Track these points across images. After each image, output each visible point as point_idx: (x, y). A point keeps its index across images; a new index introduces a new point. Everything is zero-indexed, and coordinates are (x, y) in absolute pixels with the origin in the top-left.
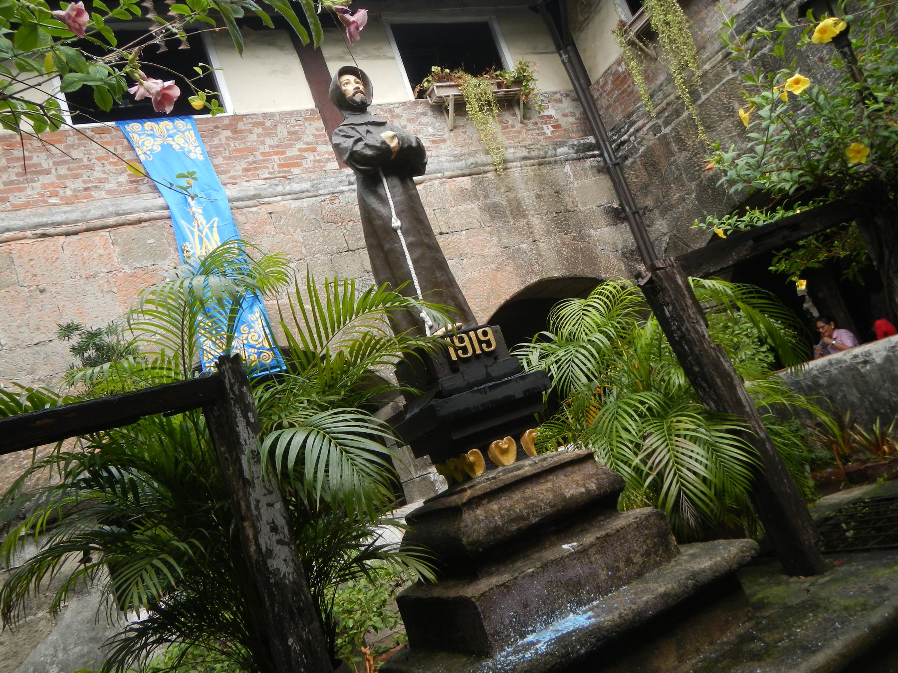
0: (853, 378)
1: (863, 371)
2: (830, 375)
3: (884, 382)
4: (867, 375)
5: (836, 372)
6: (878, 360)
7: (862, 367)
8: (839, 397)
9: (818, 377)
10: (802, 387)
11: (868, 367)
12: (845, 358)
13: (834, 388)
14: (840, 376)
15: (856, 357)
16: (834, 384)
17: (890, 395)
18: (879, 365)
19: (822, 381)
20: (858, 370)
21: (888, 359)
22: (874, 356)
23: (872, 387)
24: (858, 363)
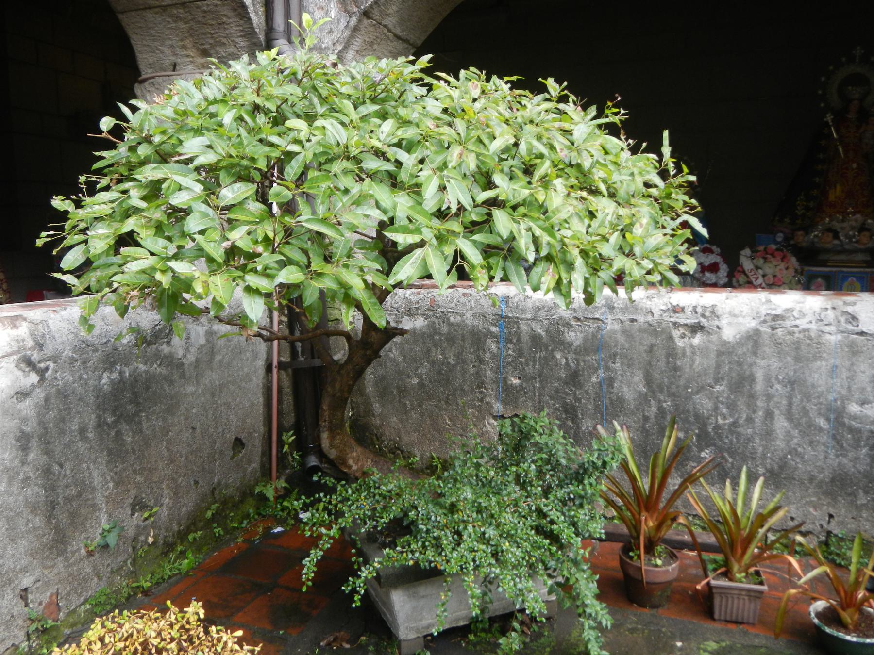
0: (651, 349)
1: (680, 343)
2: (599, 329)
3: (717, 380)
4: (684, 354)
5: (617, 327)
6: (729, 334)
7: (683, 336)
8: (594, 379)
9: (568, 325)
10: (518, 334)
11: (697, 340)
12: (648, 304)
13: (592, 358)
14: (621, 339)
15: (677, 310)
16: (597, 350)
17: (716, 408)
18: (726, 343)
19: (574, 337)
20: (671, 338)
21: (753, 338)
22: (724, 322)
23: (682, 382)
24: (675, 324)
